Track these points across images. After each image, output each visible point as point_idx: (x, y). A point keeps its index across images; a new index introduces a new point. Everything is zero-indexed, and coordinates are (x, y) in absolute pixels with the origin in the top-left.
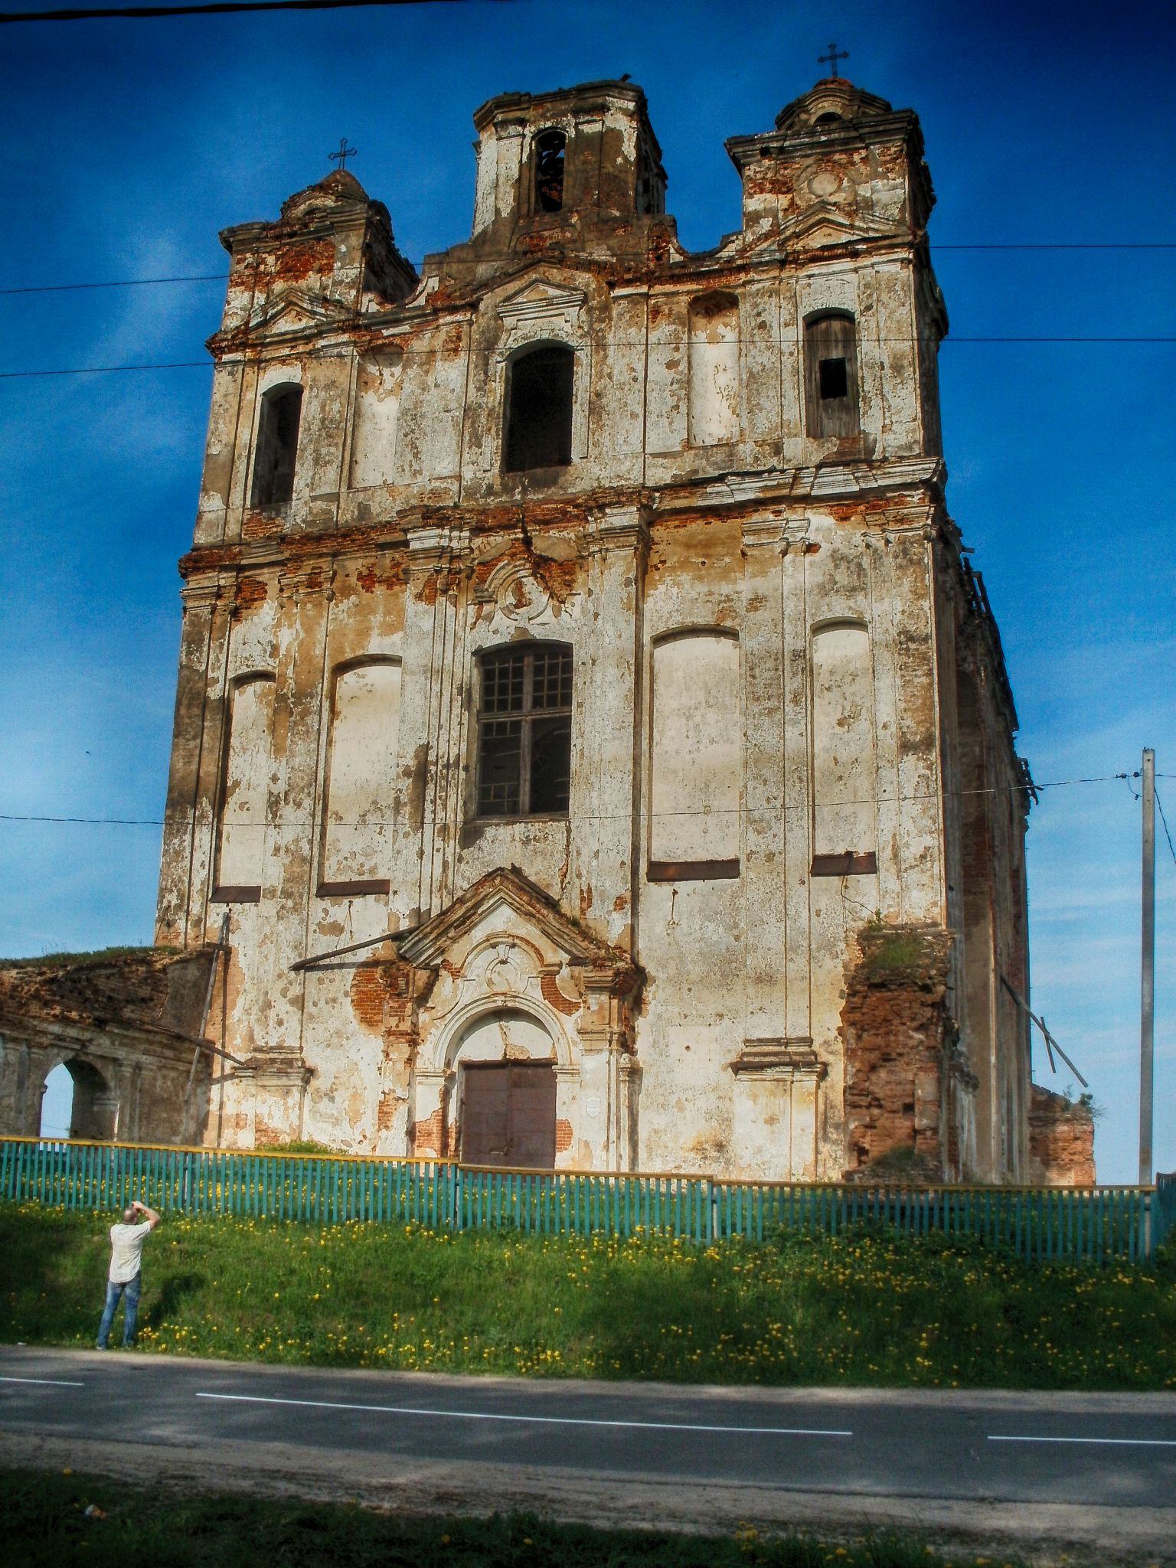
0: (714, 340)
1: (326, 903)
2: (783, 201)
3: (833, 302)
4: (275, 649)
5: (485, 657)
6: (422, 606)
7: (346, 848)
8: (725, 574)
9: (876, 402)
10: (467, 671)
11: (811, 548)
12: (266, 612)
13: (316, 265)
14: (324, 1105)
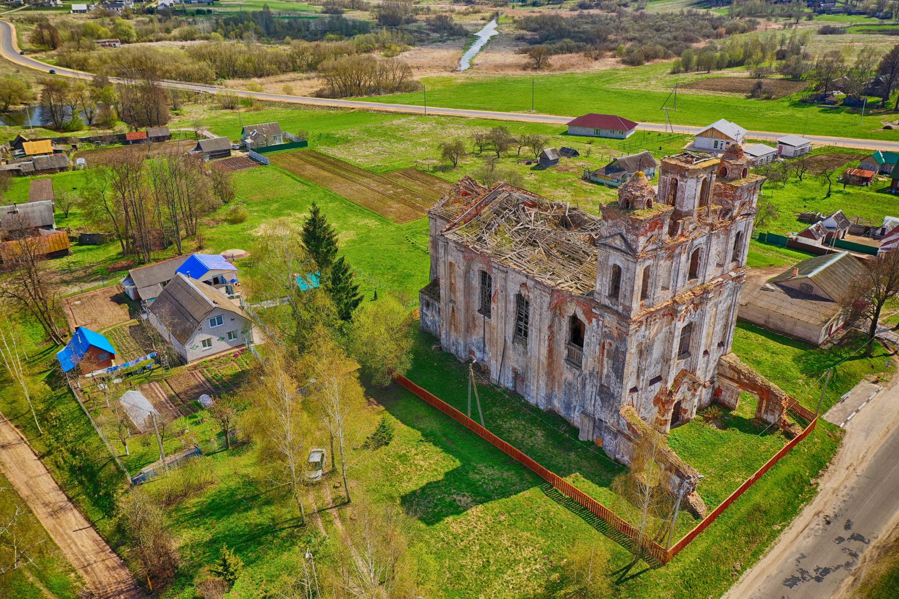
2: (739, 202)
4: (644, 336)
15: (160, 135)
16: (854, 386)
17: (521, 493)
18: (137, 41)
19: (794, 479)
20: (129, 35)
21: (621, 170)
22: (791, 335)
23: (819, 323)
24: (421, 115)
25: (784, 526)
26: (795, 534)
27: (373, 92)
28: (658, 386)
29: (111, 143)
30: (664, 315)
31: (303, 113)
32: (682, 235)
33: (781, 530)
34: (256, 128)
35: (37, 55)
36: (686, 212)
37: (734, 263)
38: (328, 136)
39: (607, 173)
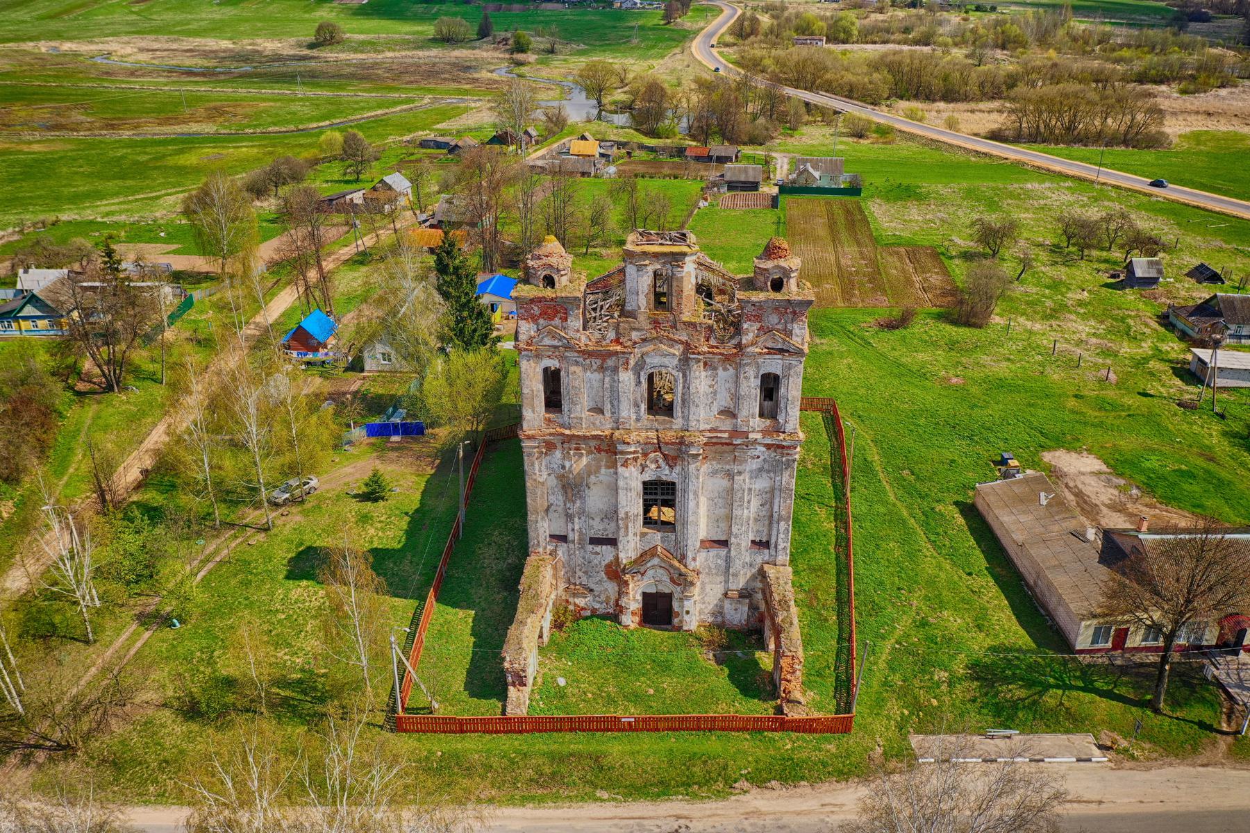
0: (725, 369)
1: (591, 546)
2: (757, 325)
3: (772, 370)
4: (564, 467)
5: (644, 483)
6: (624, 469)
7: (596, 528)
8: (727, 463)
9: (784, 411)
10: (640, 487)
11: (758, 457)
12: (558, 454)
13: (559, 315)
14: (597, 599)
15: (723, 154)
16: (1054, 732)
17: (397, 599)
18: (857, 42)
19: (705, 762)
20: (847, 32)
21: (1219, 314)
22: (1053, 619)
23: (1085, 612)
24: (1092, 182)
25: (614, 799)
26: (609, 814)
27: (1080, 141)
28: (607, 553)
29: (672, 156)
30: (599, 450)
31: (961, 157)
32: (617, 341)
33: (602, 800)
34: (811, 161)
35: (726, 49)
36: (629, 312)
37: (768, 422)
38: (908, 188)
39: (1191, 315)
